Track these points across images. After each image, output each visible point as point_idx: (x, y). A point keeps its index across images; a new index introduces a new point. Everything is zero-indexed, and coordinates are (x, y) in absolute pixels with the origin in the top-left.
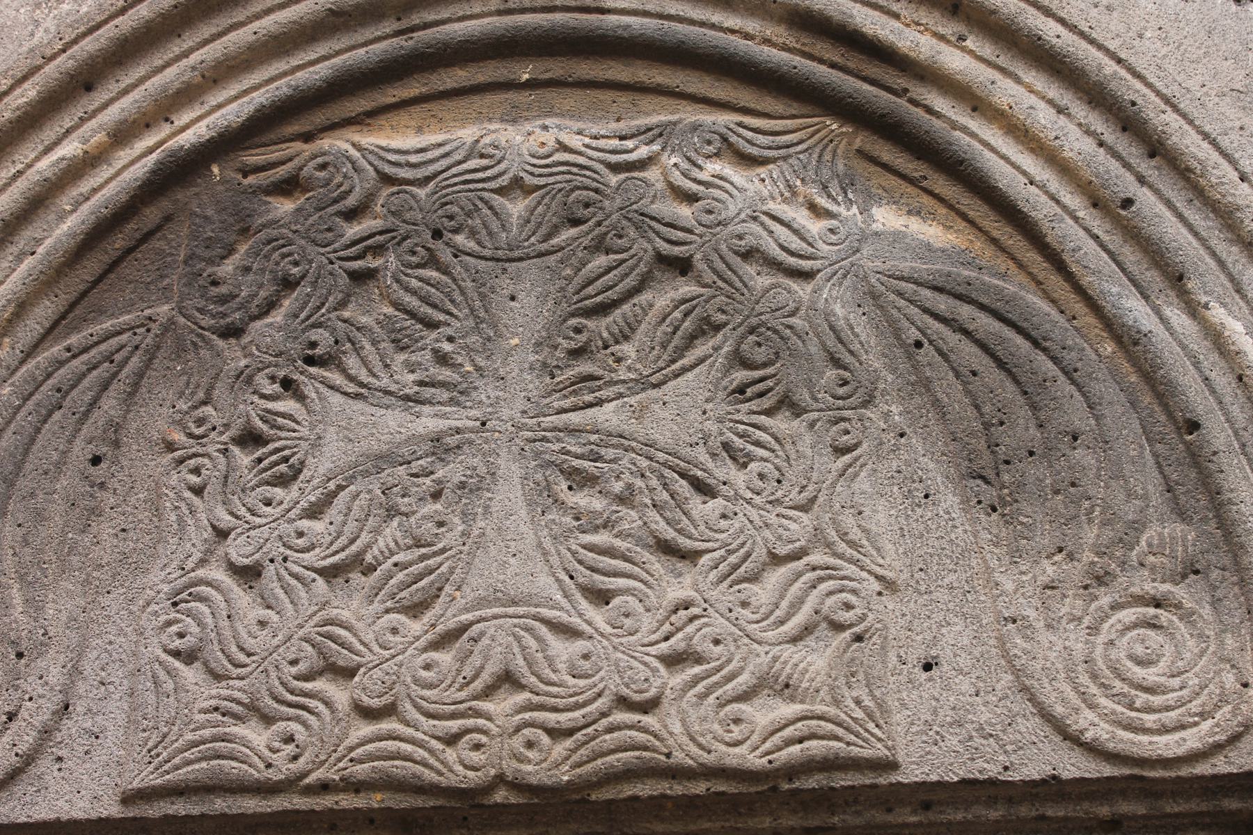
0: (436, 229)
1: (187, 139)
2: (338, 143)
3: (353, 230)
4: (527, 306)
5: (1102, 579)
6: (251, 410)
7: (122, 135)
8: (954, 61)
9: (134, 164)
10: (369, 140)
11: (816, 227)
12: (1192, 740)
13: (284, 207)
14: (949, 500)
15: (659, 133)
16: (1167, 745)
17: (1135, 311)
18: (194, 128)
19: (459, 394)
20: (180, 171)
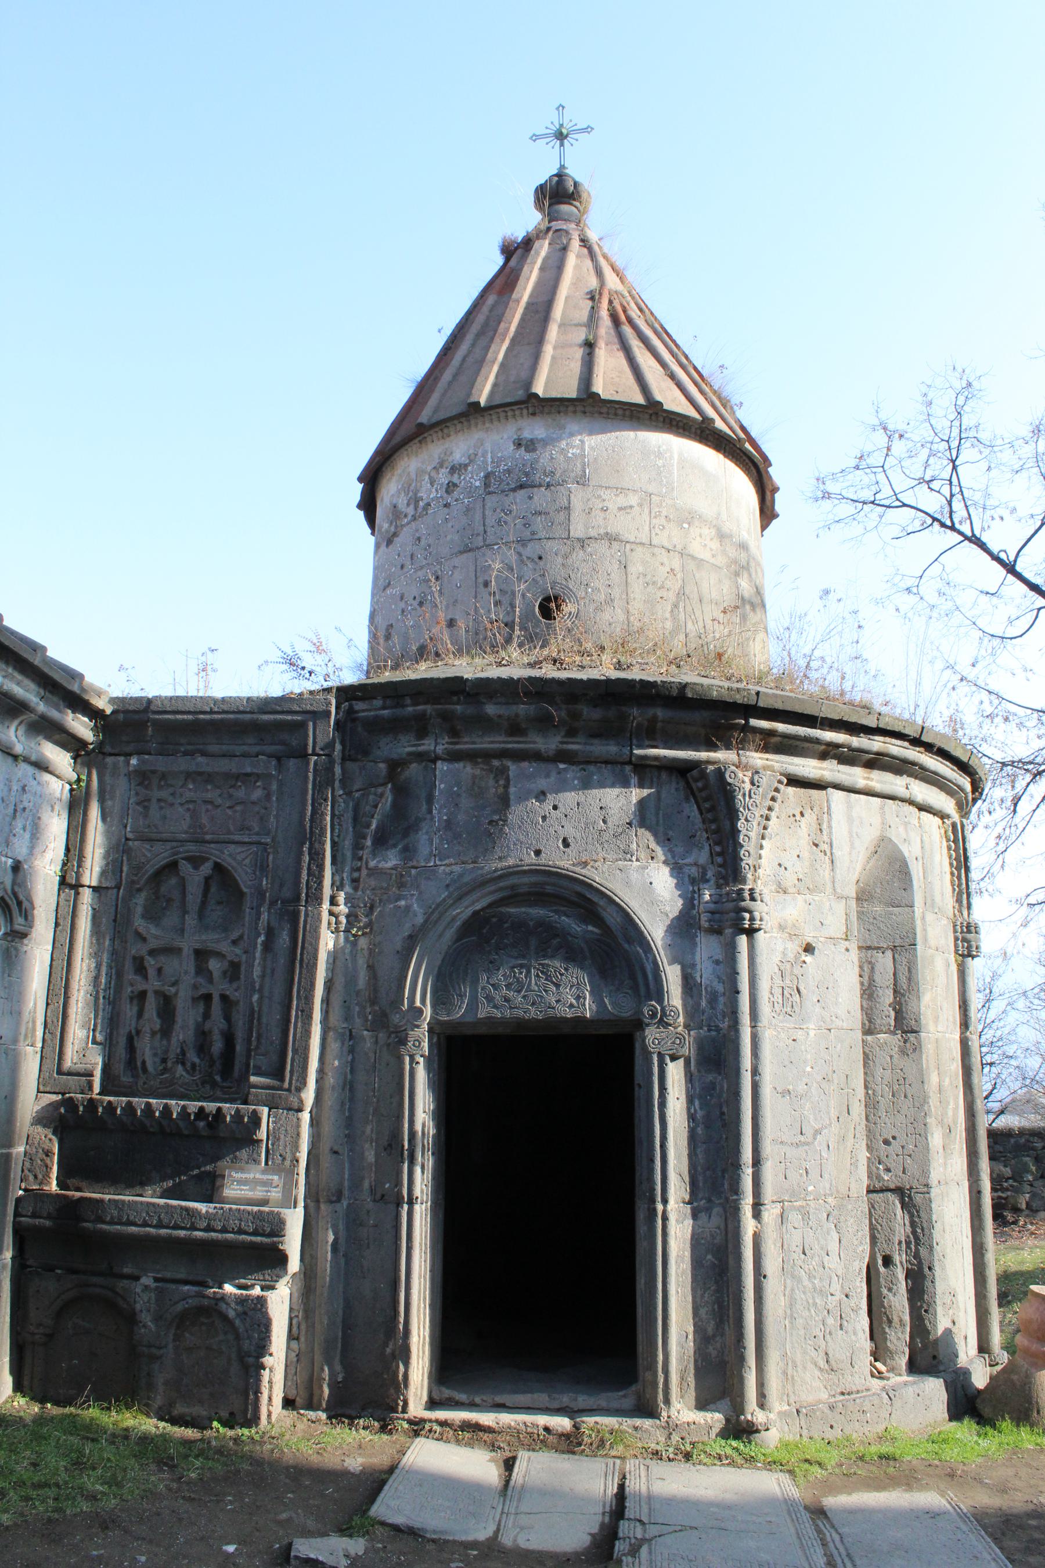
0: (519, 925)
1: (477, 908)
2: (504, 909)
3: (506, 925)
4: (533, 942)
5: (618, 989)
6: (492, 957)
7: (466, 908)
8: (602, 903)
9: (469, 912)
10: (508, 910)
11: (579, 929)
12: (628, 1014)
13: (494, 920)
14: (597, 977)
15: (556, 912)
16: (624, 1015)
17: (626, 946)
18: (478, 906)
19: (524, 957)
20: (476, 913)
